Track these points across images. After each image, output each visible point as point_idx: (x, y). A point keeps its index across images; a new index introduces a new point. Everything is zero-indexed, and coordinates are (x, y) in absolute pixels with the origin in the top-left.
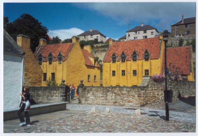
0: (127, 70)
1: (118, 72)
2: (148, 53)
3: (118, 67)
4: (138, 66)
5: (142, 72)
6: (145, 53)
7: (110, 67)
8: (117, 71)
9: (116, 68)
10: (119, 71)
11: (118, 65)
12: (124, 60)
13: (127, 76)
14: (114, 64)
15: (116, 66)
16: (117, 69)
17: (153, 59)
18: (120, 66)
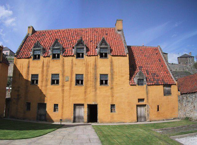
0: (63, 71)
1: (44, 77)
2: (106, 44)
3: (45, 68)
4: (87, 66)
5: (96, 79)
6: (101, 45)
7: (29, 67)
8: (43, 76)
9: (41, 70)
10: (47, 75)
11: (45, 64)
12: (59, 55)
13: (63, 86)
14: (35, 61)
15: (41, 64)
16: (43, 71)
17: (117, 56)
18: (48, 66)
